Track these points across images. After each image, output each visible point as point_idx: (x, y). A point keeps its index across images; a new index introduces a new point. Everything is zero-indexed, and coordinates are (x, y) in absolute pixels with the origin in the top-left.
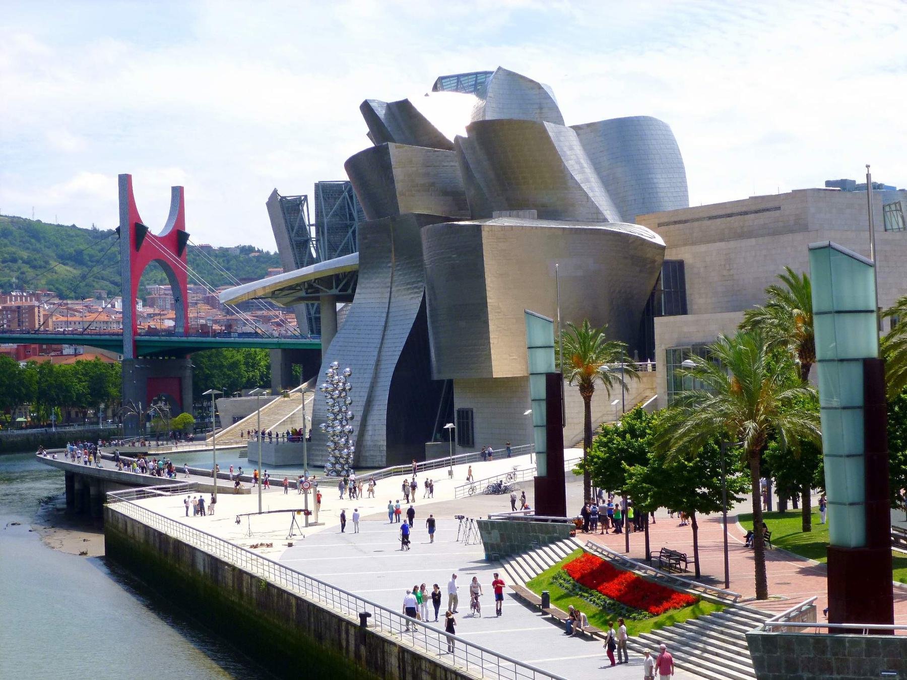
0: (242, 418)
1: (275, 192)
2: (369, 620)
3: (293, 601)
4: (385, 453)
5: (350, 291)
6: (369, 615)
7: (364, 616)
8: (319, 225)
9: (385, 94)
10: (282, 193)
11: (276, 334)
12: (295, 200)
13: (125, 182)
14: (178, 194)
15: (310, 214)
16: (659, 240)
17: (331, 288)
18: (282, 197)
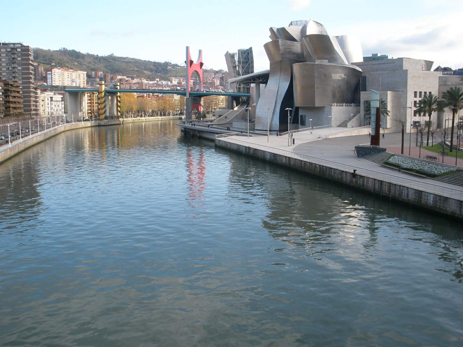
0: (222, 115)
1: (228, 52)
2: (356, 172)
3: (318, 166)
4: (278, 127)
5: (265, 81)
6: (356, 170)
7: (355, 171)
8: (239, 62)
9: (277, 26)
10: (230, 52)
11: (217, 91)
12: (233, 54)
13: (187, 48)
14: (200, 51)
15: (236, 59)
16: (360, 70)
17: (259, 79)
18: (230, 54)
